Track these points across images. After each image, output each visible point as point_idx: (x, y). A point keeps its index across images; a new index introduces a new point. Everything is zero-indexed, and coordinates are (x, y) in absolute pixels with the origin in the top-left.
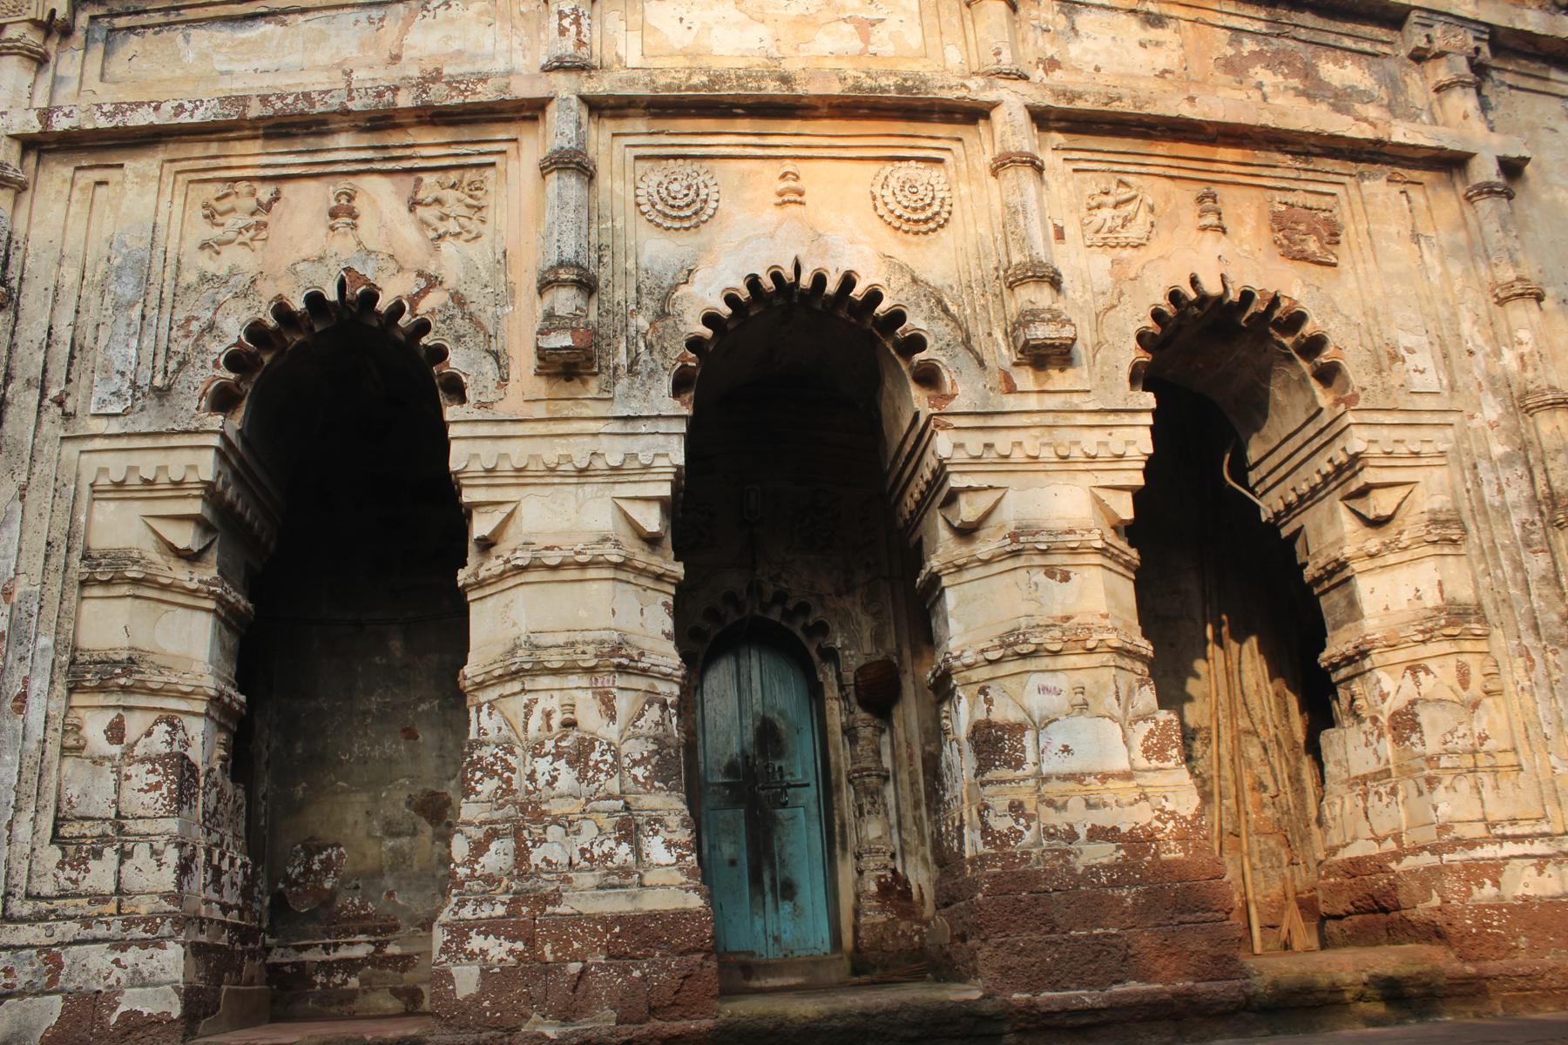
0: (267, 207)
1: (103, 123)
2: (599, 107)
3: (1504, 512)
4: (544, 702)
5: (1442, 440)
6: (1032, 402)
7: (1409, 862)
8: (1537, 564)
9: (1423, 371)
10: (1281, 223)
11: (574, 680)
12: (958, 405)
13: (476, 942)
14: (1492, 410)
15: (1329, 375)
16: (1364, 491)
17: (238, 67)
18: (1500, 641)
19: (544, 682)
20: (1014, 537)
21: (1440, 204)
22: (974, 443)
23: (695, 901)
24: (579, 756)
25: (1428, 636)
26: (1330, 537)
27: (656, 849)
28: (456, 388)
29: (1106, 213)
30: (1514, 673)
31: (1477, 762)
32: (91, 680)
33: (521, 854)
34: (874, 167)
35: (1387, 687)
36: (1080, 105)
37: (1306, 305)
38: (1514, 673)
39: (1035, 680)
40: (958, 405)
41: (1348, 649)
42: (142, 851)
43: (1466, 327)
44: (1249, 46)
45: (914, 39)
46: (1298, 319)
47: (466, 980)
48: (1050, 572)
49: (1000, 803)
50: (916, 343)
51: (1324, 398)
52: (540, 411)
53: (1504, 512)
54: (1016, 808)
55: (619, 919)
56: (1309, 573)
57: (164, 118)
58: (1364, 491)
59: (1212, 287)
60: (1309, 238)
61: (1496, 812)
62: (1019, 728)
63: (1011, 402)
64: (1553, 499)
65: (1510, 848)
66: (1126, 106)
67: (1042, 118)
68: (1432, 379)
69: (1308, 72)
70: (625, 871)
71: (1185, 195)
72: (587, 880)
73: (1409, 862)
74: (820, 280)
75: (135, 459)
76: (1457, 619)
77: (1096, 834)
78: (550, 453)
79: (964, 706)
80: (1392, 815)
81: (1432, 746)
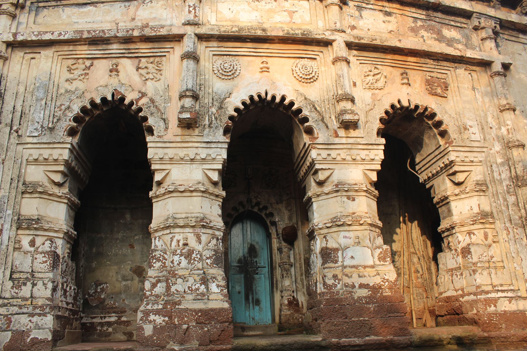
0: (89, 68)
1: (34, 38)
2: (201, 38)
3: (501, 182)
4: (177, 237)
5: (481, 157)
6: (344, 141)
7: (466, 298)
8: (512, 199)
9: (475, 133)
10: (429, 83)
11: (187, 230)
12: (319, 141)
13: (152, 317)
14: (498, 147)
15: (443, 134)
16: (454, 173)
17: (80, 21)
18: (499, 225)
19: (178, 230)
20: (337, 185)
21: (482, 78)
22: (324, 154)
23: (226, 305)
24: (188, 255)
25: (474, 222)
26: (442, 188)
27: (213, 287)
28: (151, 131)
29: (370, 78)
30: (503, 235)
31: (490, 265)
32: (24, 225)
33: (168, 288)
34: (293, 60)
35: (460, 239)
36: (362, 41)
37: (436, 111)
38: (503, 235)
39: (342, 234)
40: (319, 141)
41: (448, 226)
42: (40, 283)
43: (490, 119)
44: (419, 23)
45: (307, 18)
46: (434, 115)
47: (148, 330)
48: (348, 198)
49: (330, 275)
50: (306, 120)
51: (442, 142)
52: (178, 139)
53: (501, 182)
54: (335, 277)
55: (201, 310)
56: (435, 200)
57: (55, 37)
58: (454, 173)
59: (405, 104)
60: (438, 88)
61: (495, 282)
62: (336, 250)
63: (337, 140)
64: (517, 177)
65: (500, 294)
66: (378, 42)
67: (350, 45)
69: (439, 33)
70: (203, 295)
71: (397, 73)
72: (190, 297)
73: (466, 298)
74: (274, 98)
75: (42, 151)
76: (484, 217)
77: (362, 286)
78: (182, 153)
79: (318, 242)
80: (461, 282)
81: (475, 259)
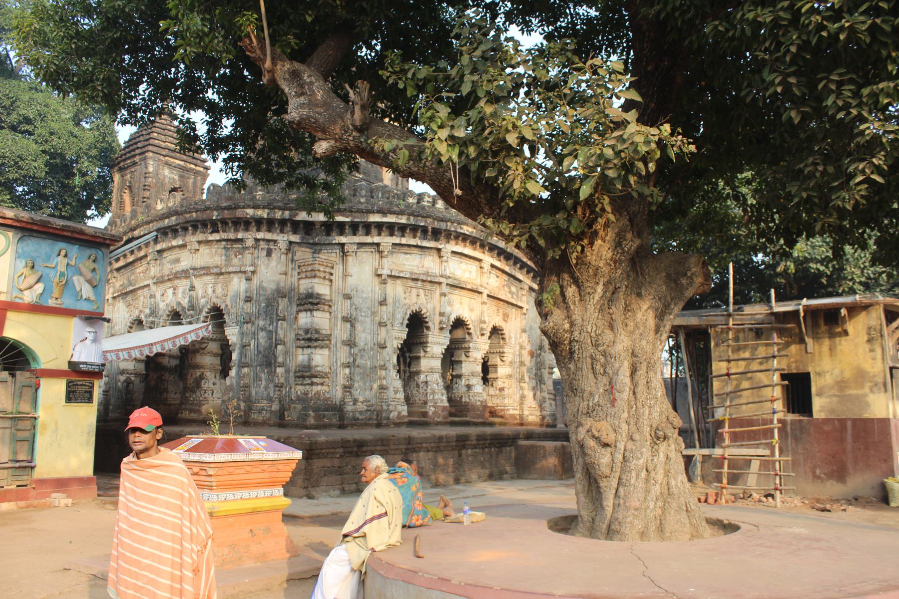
2: (447, 284)
14: (518, 348)
28: (428, 328)
31: (509, 397)
35: (499, 384)
60: (506, 317)
67: (489, 296)
68: (513, 342)
76: (510, 376)
